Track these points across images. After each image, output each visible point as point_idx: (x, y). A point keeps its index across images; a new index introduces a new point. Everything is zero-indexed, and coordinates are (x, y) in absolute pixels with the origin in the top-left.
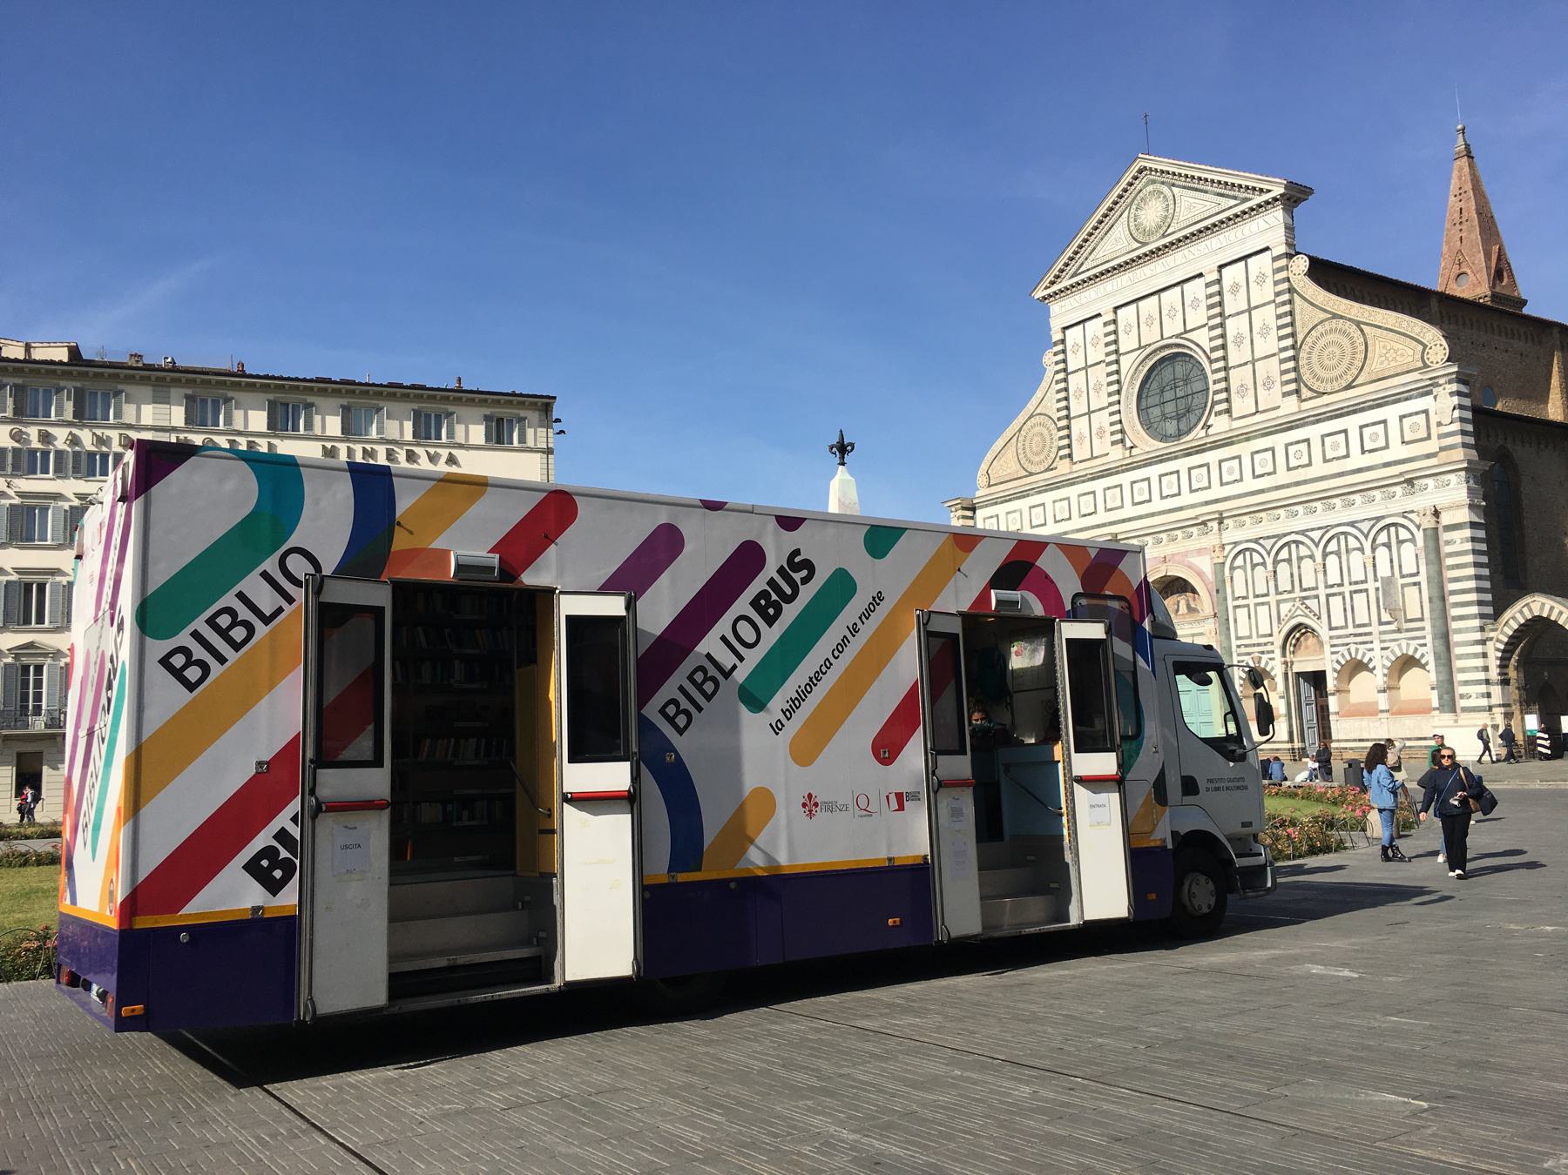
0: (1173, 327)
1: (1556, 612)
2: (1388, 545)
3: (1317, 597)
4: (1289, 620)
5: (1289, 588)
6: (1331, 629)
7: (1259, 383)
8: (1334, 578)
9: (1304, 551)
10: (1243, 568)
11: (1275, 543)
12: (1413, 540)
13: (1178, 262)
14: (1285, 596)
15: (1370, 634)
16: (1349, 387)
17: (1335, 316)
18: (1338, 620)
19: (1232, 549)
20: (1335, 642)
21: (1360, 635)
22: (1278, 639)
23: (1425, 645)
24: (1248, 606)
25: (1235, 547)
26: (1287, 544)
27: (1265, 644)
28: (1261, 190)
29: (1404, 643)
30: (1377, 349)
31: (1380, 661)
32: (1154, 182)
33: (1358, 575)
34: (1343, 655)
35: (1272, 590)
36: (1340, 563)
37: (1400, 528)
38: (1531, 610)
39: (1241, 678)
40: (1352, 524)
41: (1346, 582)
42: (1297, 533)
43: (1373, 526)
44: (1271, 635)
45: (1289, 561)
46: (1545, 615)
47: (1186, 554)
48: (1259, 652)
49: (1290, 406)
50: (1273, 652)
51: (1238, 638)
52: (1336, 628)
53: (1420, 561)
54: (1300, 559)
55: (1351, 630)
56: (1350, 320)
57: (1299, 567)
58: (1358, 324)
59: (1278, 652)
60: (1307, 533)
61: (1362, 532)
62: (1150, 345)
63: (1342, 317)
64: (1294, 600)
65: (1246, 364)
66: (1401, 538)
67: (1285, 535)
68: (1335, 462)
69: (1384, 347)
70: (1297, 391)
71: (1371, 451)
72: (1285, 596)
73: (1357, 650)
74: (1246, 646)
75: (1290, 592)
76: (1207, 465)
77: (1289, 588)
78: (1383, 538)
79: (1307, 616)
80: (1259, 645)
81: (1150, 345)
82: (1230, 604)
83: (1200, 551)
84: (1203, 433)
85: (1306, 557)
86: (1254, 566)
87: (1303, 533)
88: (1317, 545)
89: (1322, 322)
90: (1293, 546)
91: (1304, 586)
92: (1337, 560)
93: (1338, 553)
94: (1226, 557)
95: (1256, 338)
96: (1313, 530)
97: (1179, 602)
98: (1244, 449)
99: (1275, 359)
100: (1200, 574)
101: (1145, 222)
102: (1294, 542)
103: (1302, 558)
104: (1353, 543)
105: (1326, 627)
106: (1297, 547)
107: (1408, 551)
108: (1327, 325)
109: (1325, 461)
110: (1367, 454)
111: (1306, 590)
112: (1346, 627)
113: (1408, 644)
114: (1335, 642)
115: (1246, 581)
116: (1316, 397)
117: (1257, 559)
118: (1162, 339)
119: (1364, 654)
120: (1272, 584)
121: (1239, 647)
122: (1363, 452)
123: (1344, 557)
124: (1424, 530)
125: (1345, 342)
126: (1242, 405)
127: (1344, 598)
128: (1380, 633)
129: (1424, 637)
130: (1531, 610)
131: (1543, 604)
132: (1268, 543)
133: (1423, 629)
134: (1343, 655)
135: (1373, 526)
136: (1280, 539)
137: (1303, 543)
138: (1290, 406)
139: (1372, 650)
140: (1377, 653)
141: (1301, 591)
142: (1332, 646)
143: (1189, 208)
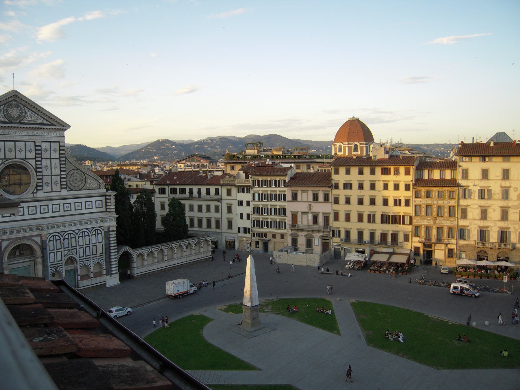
0: (20, 155)
1: (123, 250)
2: (95, 235)
3: (76, 249)
4: (69, 255)
5: (68, 246)
6: (80, 257)
7: (53, 183)
8: (81, 243)
9: (72, 236)
10: (53, 241)
11: (64, 234)
12: (101, 233)
13: (25, 134)
14: (66, 249)
15: (90, 258)
16: (80, 190)
17: (78, 169)
18: (81, 255)
19: (50, 235)
20: (81, 261)
21: (88, 258)
22: (64, 262)
23: (103, 259)
24: (54, 253)
25: (51, 234)
26: (68, 234)
27: (59, 264)
28: (61, 124)
29: (98, 259)
30: (89, 181)
31: (92, 264)
32: (16, 101)
33: (87, 242)
34: (82, 264)
35: (63, 248)
36: (83, 239)
37: (98, 230)
38: (124, 250)
39: (51, 275)
40: (87, 229)
41: (84, 244)
42: (71, 231)
43: (92, 230)
44: (62, 261)
45: (68, 239)
46: (127, 250)
47: (31, 236)
48: (57, 266)
49: (64, 193)
50: (62, 266)
51: (50, 263)
52: (81, 257)
53: (103, 239)
54: (71, 238)
55: (85, 257)
56: (82, 171)
57: (71, 241)
58: (84, 173)
59: (64, 265)
60: (75, 231)
61: (89, 231)
62: (10, 159)
63: (79, 170)
64: (69, 250)
65: (48, 175)
66: (99, 233)
67: (67, 231)
68: (78, 211)
69: (90, 181)
70: (66, 188)
71: (88, 209)
72: (66, 249)
73: (86, 262)
74: (53, 265)
75: (68, 248)
76: (36, 206)
77: (68, 246)
78: (94, 233)
79: (73, 254)
80: (57, 264)
81: (10, 159)
82: (48, 252)
83: (36, 236)
84: (31, 196)
85: (73, 237)
86: (56, 240)
87: (73, 231)
88: (77, 234)
89: (74, 169)
90: (69, 235)
91: (72, 246)
92: (82, 238)
93: (82, 237)
94: (48, 237)
95: (53, 169)
96: (76, 230)
97: (16, 252)
98: (50, 203)
99: (59, 177)
100: (37, 243)
101: (11, 114)
102: (70, 233)
103: (72, 238)
104: (86, 234)
105: (78, 257)
106: (71, 235)
107: (100, 236)
108: (75, 171)
109: (75, 210)
110: (87, 210)
111: (73, 247)
112: (84, 256)
113: (99, 260)
114: (81, 261)
115: (54, 245)
116: (71, 191)
117: (58, 238)
118: (16, 158)
119: (88, 263)
120: (62, 246)
121: (50, 265)
122: (86, 209)
123: (84, 238)
124: (105, 231)
125: (80, 177)
126: (47, 188)
127: (83, 249)
128: (93, 257)
129: (103, 258)
130: (124, 250)
131: (127, 248)
132: (62, 234)
133: (103, 255)
134: (82, 264)
135: (92, 230)
136: (66, 232)
137: (72, 234)
138: (65, 193)
139: (90, 262)
140: (92, 262)
141: (71, 247)
142: (80, 262)
143: (31, 117)
